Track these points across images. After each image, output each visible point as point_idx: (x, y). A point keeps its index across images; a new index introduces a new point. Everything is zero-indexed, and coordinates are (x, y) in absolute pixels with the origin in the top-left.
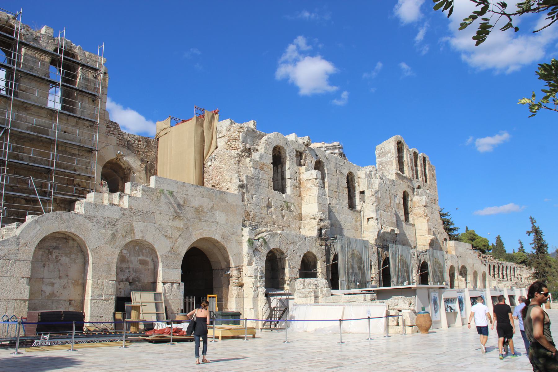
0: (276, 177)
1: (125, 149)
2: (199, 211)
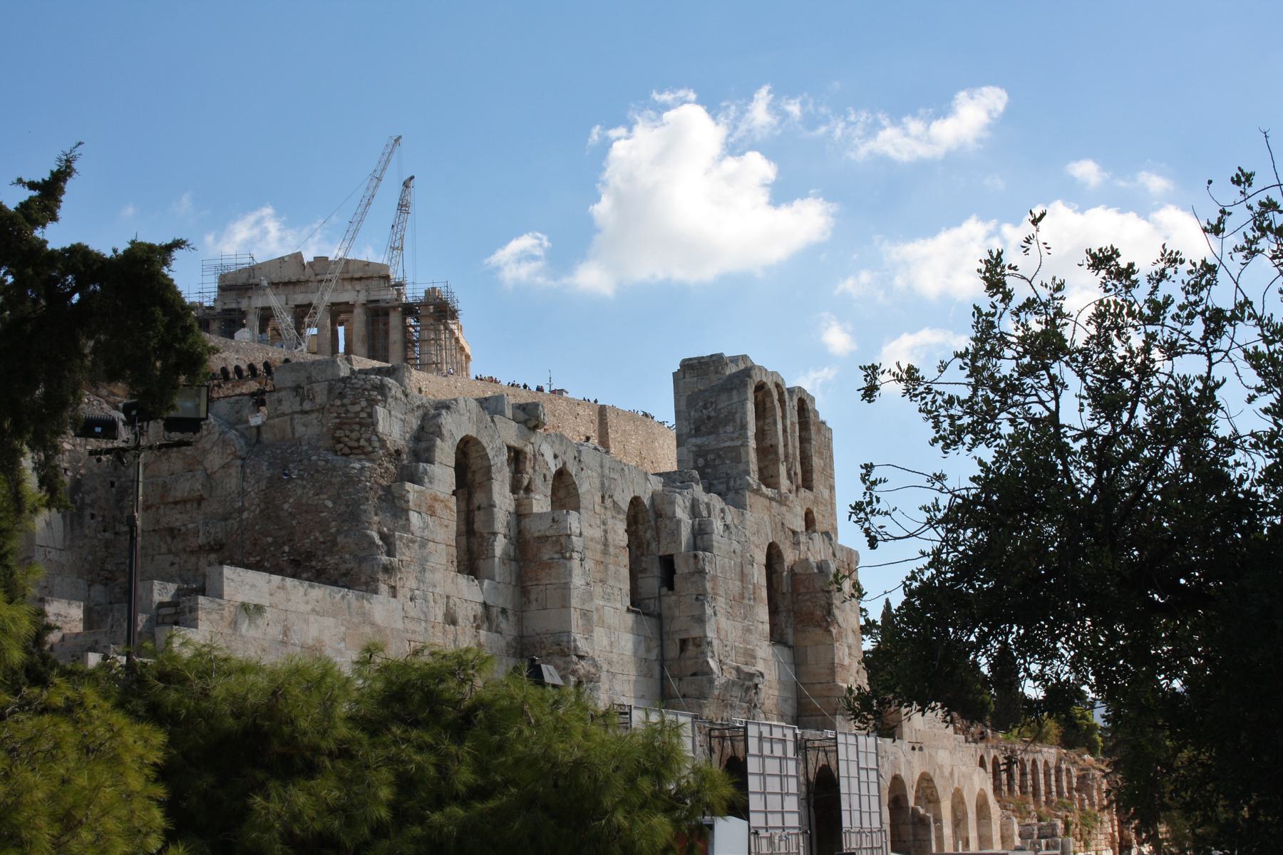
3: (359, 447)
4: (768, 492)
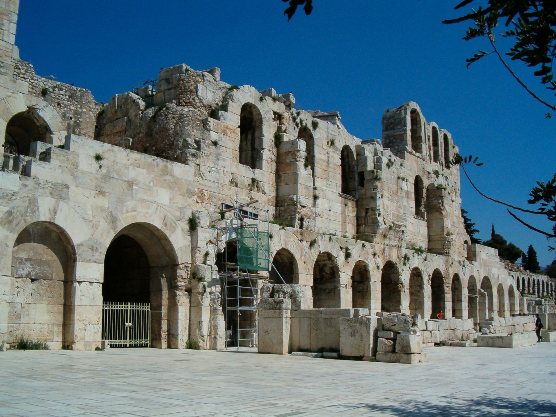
0: (244, 146)
2: (131, 184)
3: (190, 102)
4: (418, 154)
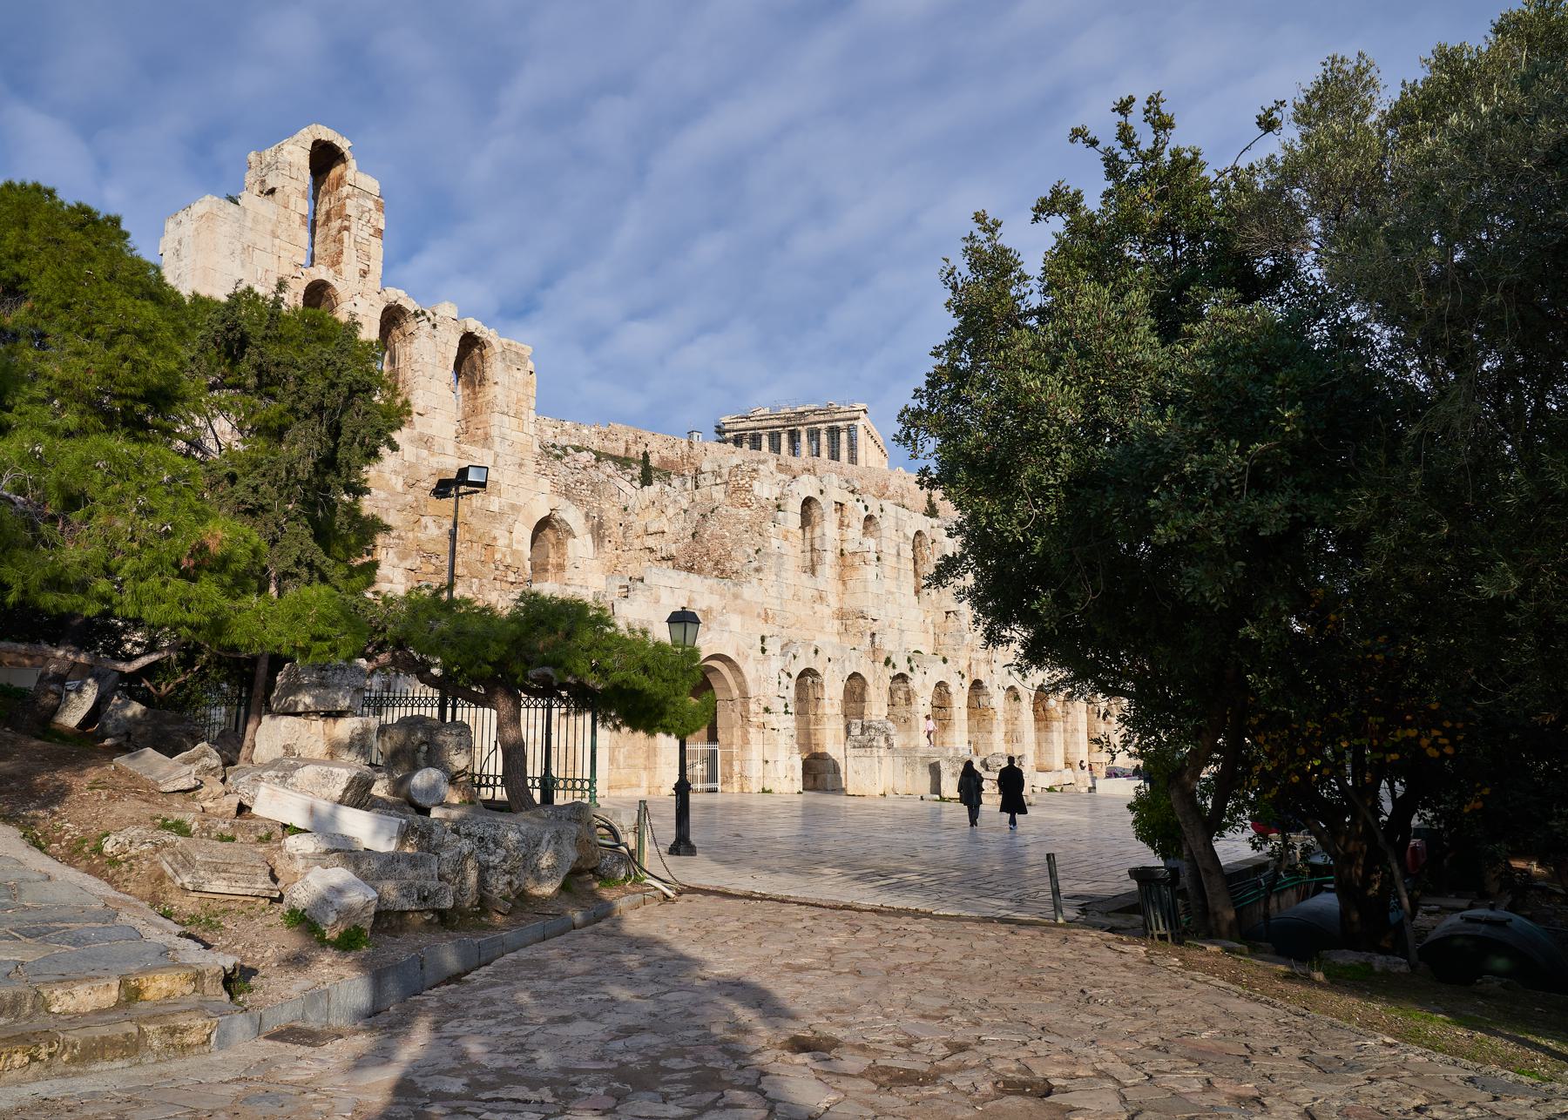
1: (563, 499)
